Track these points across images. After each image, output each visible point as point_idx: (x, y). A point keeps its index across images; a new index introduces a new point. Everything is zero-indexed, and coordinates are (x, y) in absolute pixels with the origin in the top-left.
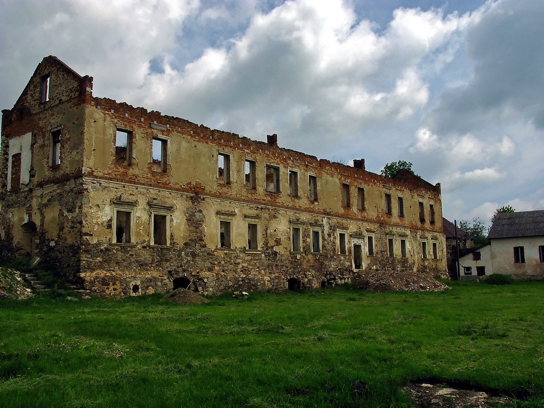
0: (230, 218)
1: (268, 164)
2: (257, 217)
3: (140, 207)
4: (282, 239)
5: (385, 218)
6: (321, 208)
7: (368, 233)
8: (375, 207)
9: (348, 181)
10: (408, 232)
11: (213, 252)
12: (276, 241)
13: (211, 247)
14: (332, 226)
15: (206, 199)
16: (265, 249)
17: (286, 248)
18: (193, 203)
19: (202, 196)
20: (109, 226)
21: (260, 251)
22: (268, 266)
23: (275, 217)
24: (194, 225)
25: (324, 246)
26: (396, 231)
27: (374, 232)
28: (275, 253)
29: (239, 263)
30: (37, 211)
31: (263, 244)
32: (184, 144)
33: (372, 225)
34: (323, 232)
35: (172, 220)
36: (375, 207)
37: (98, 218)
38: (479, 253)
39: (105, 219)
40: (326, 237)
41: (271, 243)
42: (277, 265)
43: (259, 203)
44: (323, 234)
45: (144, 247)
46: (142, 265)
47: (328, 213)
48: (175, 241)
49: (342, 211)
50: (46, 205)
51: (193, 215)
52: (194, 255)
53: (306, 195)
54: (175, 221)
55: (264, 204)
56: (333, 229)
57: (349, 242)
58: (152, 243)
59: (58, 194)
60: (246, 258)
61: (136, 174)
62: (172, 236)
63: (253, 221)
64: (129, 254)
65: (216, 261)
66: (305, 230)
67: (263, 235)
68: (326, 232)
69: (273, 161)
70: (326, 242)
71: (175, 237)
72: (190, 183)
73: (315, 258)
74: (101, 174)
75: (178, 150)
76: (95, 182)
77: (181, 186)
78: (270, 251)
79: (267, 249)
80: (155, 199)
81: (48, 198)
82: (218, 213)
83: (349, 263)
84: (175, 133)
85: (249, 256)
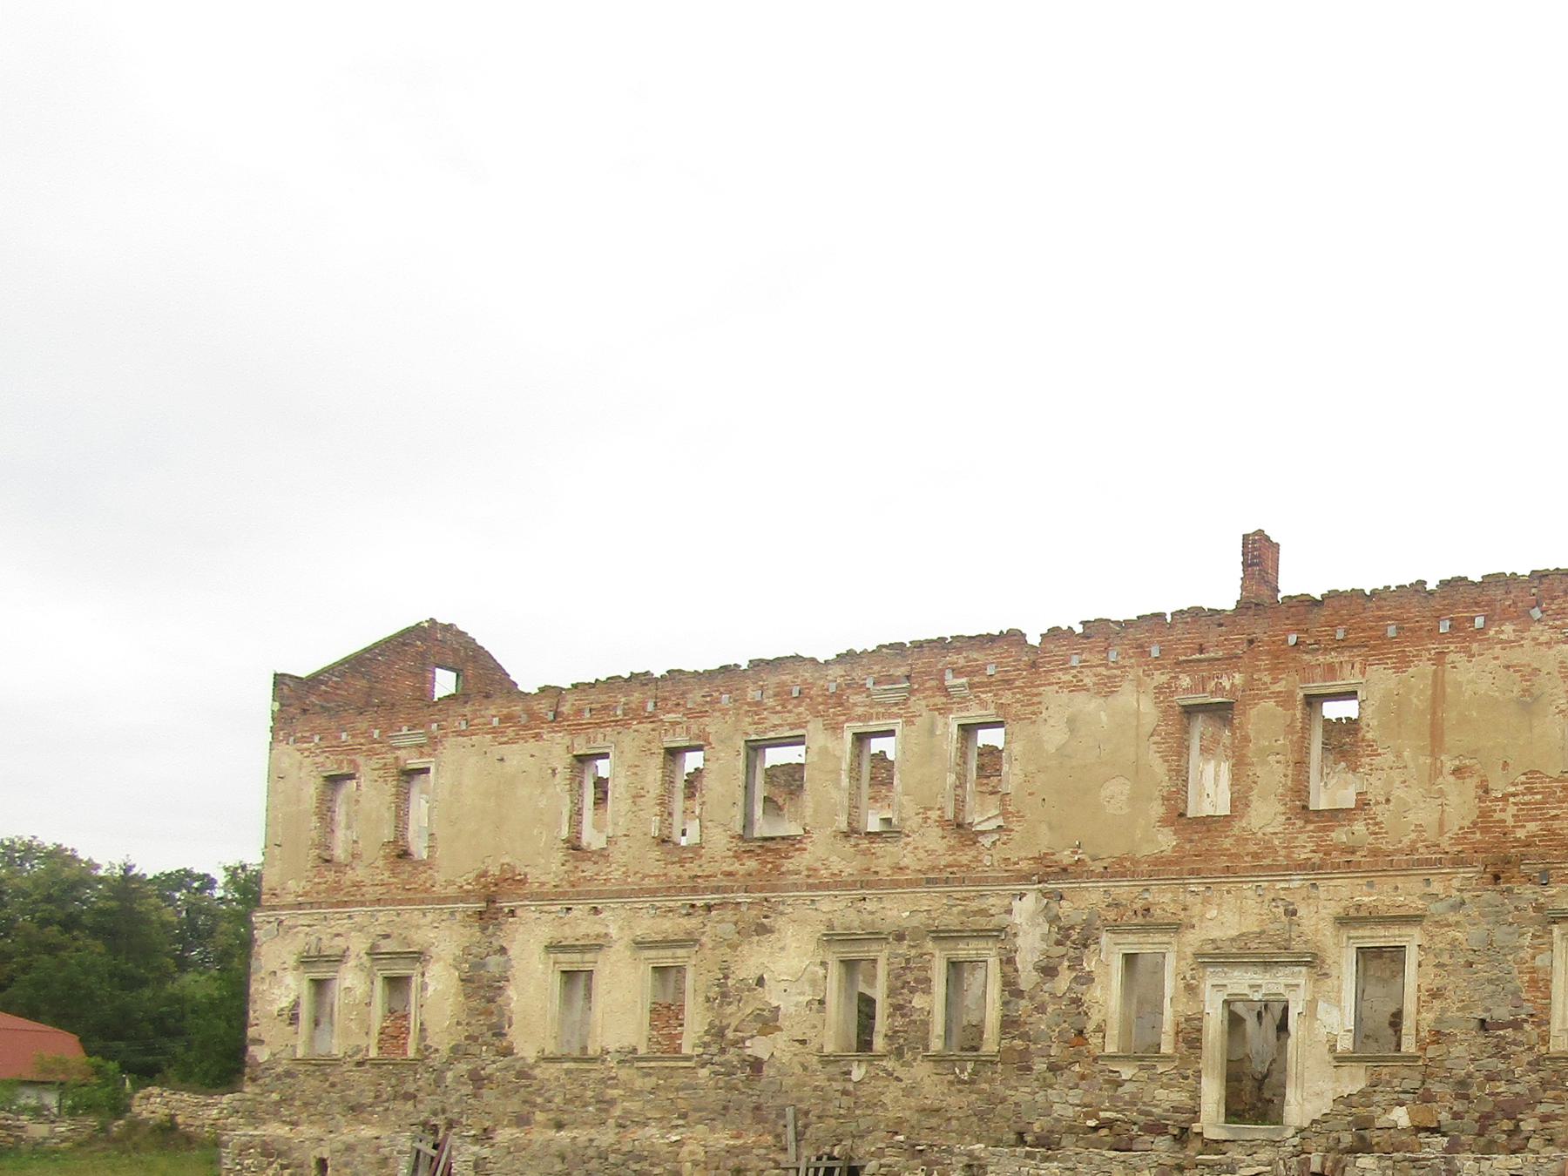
0: (589, 957)
1: (754, 737)
2: (689, 941)
3: (352, 963)
5: (1556, 824)
6: (1023, 854)
7: (1353, 933)
8: (1458, 772)
11: (532, 1067)
13: (527, 1050)
14: (1072, 927)
15: (518, 912)
16: (714, 1049)
18: (484, 929)
19: (506, 906)
20: (294, 1019)
21: (688, 1058)
22: (725, 1108)
23: (763, 930)
24: (482, 993)
25: (1009, 1024)
28: (757, 1065)
29: (612, 1102)
31: (707, 1032)
35: (424, 987)
36: (1458, 772)
37: (272, 1002)
39: (285, 1003)
40: (1027, 978)
42: (758, 1108)
43: (694, 890)
44: (1009, 969)
46: (352, 1109)
47: (1065, 870)
48: (428, 1042)
49: (1166, 841)
51: (480, 965)
52: (477, 1079)
53: (934, 815)
54: (430, 989)
55: (716, 890)
57: (1191, 990)
58: (373, 1053)
62: (423, 1030)
63: (665, 957)
64: (328, 1083)
65: (540, 1095)
66: (908, 961)
67: (708, 1000)
69: (776, 720)
70: (1023, 1003)
71: (430, 1032)
72: (484, 874)
73: (951, 1077)
77: (461, 887)
78: (731, 1055)
79: (723, 1051)
80: (387, 936)
83: (1179, 1097)
84: (451, 741)
85: (649, 1075)
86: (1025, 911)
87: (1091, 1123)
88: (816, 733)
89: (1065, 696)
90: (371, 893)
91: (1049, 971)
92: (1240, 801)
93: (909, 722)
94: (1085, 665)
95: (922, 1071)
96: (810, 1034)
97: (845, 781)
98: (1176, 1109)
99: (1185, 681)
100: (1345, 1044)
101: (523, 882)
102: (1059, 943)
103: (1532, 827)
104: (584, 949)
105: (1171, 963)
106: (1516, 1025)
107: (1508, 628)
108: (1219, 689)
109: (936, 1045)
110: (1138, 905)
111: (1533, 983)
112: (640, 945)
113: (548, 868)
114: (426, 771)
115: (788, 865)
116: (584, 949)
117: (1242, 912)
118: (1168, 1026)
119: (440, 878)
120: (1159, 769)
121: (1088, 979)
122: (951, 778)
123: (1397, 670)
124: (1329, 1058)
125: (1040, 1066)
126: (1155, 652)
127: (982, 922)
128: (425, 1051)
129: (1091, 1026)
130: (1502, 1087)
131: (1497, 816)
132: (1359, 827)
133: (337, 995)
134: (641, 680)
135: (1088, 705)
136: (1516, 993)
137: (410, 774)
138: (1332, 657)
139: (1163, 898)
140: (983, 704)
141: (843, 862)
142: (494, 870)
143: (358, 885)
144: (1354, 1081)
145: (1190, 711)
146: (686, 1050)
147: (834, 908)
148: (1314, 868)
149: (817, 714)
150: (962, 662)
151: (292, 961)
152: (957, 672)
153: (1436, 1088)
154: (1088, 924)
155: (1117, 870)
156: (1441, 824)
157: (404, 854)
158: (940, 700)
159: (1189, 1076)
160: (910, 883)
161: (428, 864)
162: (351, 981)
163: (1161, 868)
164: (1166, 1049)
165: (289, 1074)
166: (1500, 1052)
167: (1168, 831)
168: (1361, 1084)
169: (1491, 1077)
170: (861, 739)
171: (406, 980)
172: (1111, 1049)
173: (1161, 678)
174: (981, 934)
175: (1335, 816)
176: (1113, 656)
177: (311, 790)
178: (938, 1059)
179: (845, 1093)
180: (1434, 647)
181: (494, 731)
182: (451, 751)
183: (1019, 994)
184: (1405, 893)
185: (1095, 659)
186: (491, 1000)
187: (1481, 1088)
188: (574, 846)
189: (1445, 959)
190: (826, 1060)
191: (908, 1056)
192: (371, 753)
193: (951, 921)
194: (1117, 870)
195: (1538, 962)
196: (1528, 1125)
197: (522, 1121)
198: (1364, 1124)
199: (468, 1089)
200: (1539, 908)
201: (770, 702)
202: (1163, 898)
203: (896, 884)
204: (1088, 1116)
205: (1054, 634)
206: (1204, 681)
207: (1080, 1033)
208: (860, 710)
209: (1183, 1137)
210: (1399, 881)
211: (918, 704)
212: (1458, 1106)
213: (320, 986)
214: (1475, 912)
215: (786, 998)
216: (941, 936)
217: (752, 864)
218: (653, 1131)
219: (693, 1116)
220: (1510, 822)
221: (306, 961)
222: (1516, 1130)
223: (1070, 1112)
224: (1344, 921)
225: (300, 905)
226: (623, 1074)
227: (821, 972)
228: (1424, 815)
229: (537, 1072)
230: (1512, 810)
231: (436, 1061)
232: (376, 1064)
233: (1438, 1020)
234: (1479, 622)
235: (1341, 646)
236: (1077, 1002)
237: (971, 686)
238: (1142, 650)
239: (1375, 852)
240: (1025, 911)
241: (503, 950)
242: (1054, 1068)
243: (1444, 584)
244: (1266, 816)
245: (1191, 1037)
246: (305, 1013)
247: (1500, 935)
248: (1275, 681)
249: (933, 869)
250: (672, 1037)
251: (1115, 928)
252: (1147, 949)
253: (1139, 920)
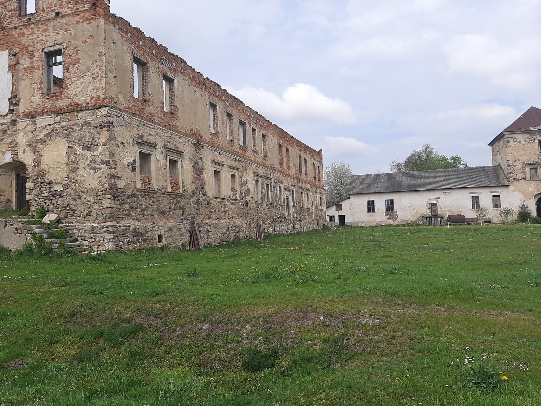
9: (281, 142)
11: (211, 200)
15: (204, 147)
20: (134, 169)
30: (27, 149)
35: (182, 167)
38: (341, 205)
39: (131, 160)
43: (237, 155)
45: (163, 194)
46: (162, 213)
48: (185, 188)
50: (43, 141)
54: (184, 167)
58: (169, 190)
59: (63, 127)
61: (152, 112)
65: (213, 209)
71: (185, 184)
74: (122, 107)
75: (183, 92)
76: (119, 115)
81: (45, 132)
112: (230, 167)
171: (177, 161)
199: (196, 206)
213: (145, 157)
219: (240, 216)
226: (228, 203)
232: (170, 194)
241: (201, 158)
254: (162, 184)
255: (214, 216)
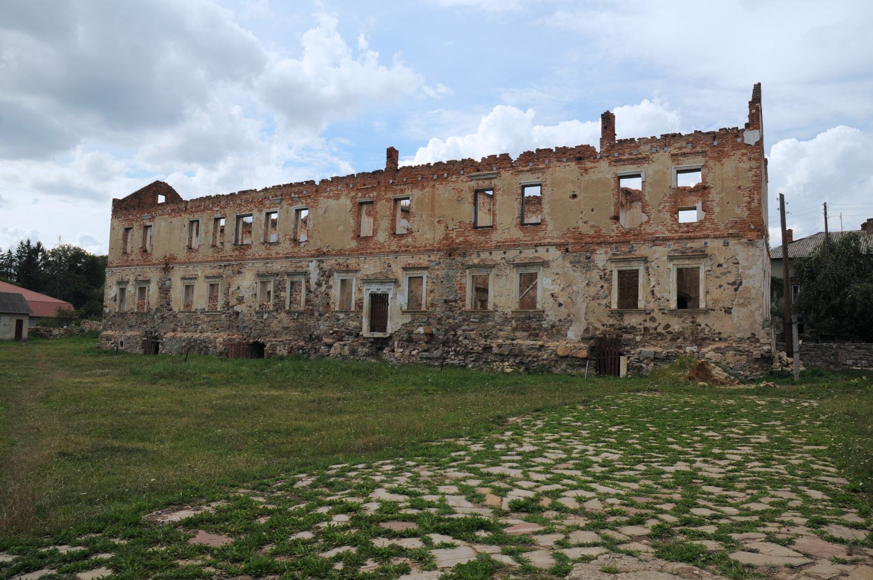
0: (193, 281)
2: (220, 276)
3: (131, 283)
4: (246, 297)
8: (439, 222)
10: (554, 254)
12: (238, 299)
13: (176, 309)
16: (226, 309)
17: (250, 307)
18: (165, 273)
20: (115, 300)
23: (239, 272)
25: (308, 301)
26: (504, 258)
27: (426, 268)
28: (237, 314)
29: (198, 325)
32: (163, 224)
33: (426, 257)
34: (308, 282)
35: (149, 290)
39: (113, 295)
40: (313, 287)
41: (233, 301)
42: (238, 327)
43: (221, 261)
45: (132, 313)
49: (354, 244)
53: (288, 237)
56: (327, 275)
57: (360, 290)
60: (206, 319)
63: (213, 281)
68: (313, 281)
69: (244, 209)
72: (166, 257)
78: (231, 311)
79: (228, 309)
82: (183, 278)
83: (356, 324)
84: (158, 217)
86: (313, 268)
87: (331, 332)
88: (255, 212)
89: (325, 200)
90: (136, 262)
91: (319, 285)
92: (375, 232)
93: (282, 208)
94: (331, 190)
95: (283, 315)
96: (252, 304)
97: (263, 227)
98: (355, 328)
99: (360, 195)
100: (405, 308)
101: (176, 259)
102: (322, 276)
103: (461, 239)
104: (191, 279)
105: (354, 281)
106: (456, 301)
107: (454, 177)
108: (370, 197)
109: (287, 308)
110: (345, 264)
111: (461, 288)
112: (207, 277)
113: (181, 254)
114: (151, 226)
115: (247, 253)
116: (191, 279)
117: (375, 266)
118: (353, 302)
119: (154, 258)
120: (352, 222)
121: (330, 287)
122: (293, 226)
123: (421, 190)
124: (400, 312)
125: (316, 314)
126: (351, 186)
127: (299, 270)
128: (149, 310)
129: (331, 302)
130: (451, 321)
131: (450, 235)
132: (410, 239)
133: (127, 294)
134: (209, 198)
135: (332, 202)
136: (456, 291)
137: (146, 228)
138: (402, 187)
139: (352, 262)
140: (302, 203)
141: (262, 252)
142: (168, 255)
143: (132, 260)
144: (407, 319)
145: (361, 204)
146: (219, 309)
147: (260, 266)
148: (396, 252)
149: (256, 207)
150: (296, 190)
151: (115, 283)
152: (295, 193)
153: (431, 321)
154: (331, 270)
155: (340, 253)
156: (434, 238)
157: (145, 251)
158: (290, 202)
159: (358, 318)
160: (282, 258)
161: (151, 254)
162: (131, 289)
163: (352, 253)
164: (353, 309)
165: (114, 316)
166: (451, 310)
167: (355, 241)
168: (410, 320)
169: (449, 318)
170: (268, 214)
172: (337, 309)
173: (353, 194)
174: (300, 274)
175: (402, 236)
176: (339, 188)
177: (121, 232)
178: (288, 312)
179: (262, 322)
180: (432, 183)
181: (169, 214)
182: (158, 220)
183: (310, 292)
184: (423, 260)
185: (334, 188)
186: (167, 294)
187: (445, 321)
188: (190, 248)
189: (435, 280)
190: (257, 313)
191: (279, 311)
192: (137, 221)
193: (291, 270)
194: (340, 253)
195: (462, 281)
196: (459, 332)
197: (174, 330)
198: (410, 333)
200: (463, 264)
201: (243, 204)
202: (352, 262)
203: (277, 258)
204: (330, 330)
205: (323, 181)
206: (365, 194)
207: (328, 304)
208: (267, 205)
209: (358, 335)
210: (422, 256)
211: (285, 204)
212: (439, 327)
213: (123, 291)
214: (443, 266)
215: (246, 294)
216: (289, 274)
217: (237, 253)
218: (209, 334)
220: (454, 237)
221: (119, 283)
222: (455, 335)
223: (325, 328)
224: (405, 269)
225: (117, 266)
226: (202, 316)
227: (255, 285)
228: (429, 235)
229: (178, 316)
230: (455, 233)
231: (152, 312)
232: (137, 313)
233: (432, 300)
234: (445, 175)
235: (405, 183)
236: (327, 294)
237: (299, 197)
238: (347, 185)
239: (414, 247)
240: (313, 268)
241: (170, 279)
242: (320, 315)
243: (436, 164)
244: (382, 237)
245: (359, 305)
246: (118, 298)
247: (451, 273)
248: (386, 194)
249: (287, 254)
250: (215, 305)
251: (338, 272)
252: (347, 278)
253: (345, 269)
254: (132, 306)
255: (179, 329)
